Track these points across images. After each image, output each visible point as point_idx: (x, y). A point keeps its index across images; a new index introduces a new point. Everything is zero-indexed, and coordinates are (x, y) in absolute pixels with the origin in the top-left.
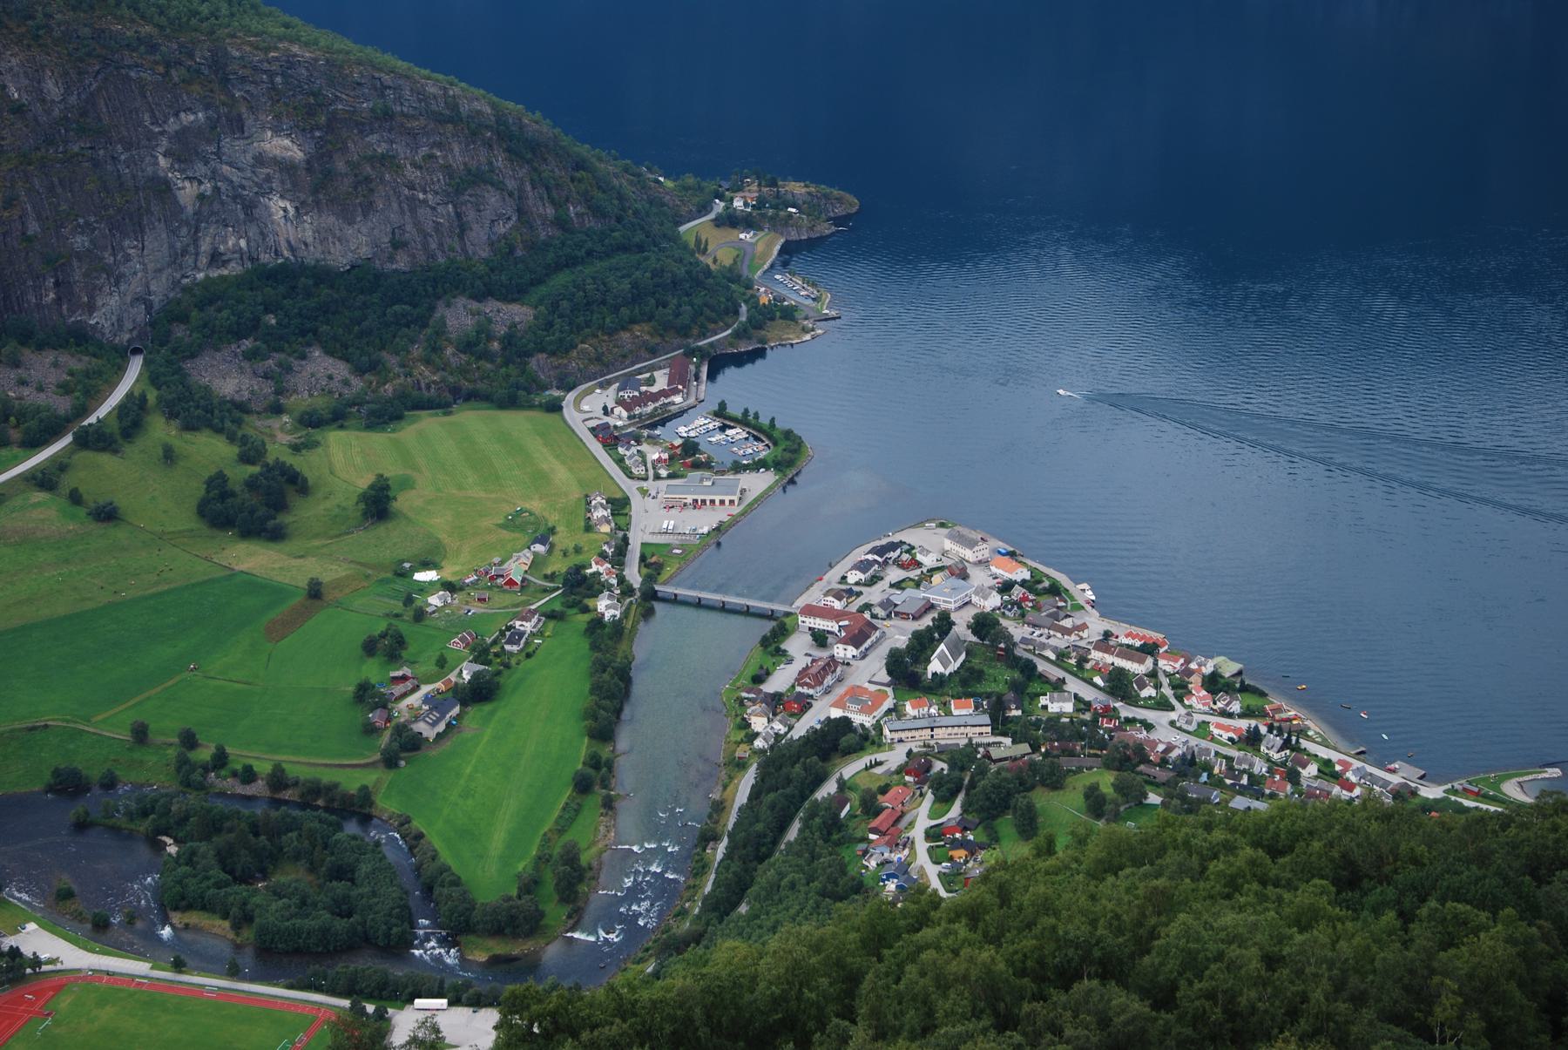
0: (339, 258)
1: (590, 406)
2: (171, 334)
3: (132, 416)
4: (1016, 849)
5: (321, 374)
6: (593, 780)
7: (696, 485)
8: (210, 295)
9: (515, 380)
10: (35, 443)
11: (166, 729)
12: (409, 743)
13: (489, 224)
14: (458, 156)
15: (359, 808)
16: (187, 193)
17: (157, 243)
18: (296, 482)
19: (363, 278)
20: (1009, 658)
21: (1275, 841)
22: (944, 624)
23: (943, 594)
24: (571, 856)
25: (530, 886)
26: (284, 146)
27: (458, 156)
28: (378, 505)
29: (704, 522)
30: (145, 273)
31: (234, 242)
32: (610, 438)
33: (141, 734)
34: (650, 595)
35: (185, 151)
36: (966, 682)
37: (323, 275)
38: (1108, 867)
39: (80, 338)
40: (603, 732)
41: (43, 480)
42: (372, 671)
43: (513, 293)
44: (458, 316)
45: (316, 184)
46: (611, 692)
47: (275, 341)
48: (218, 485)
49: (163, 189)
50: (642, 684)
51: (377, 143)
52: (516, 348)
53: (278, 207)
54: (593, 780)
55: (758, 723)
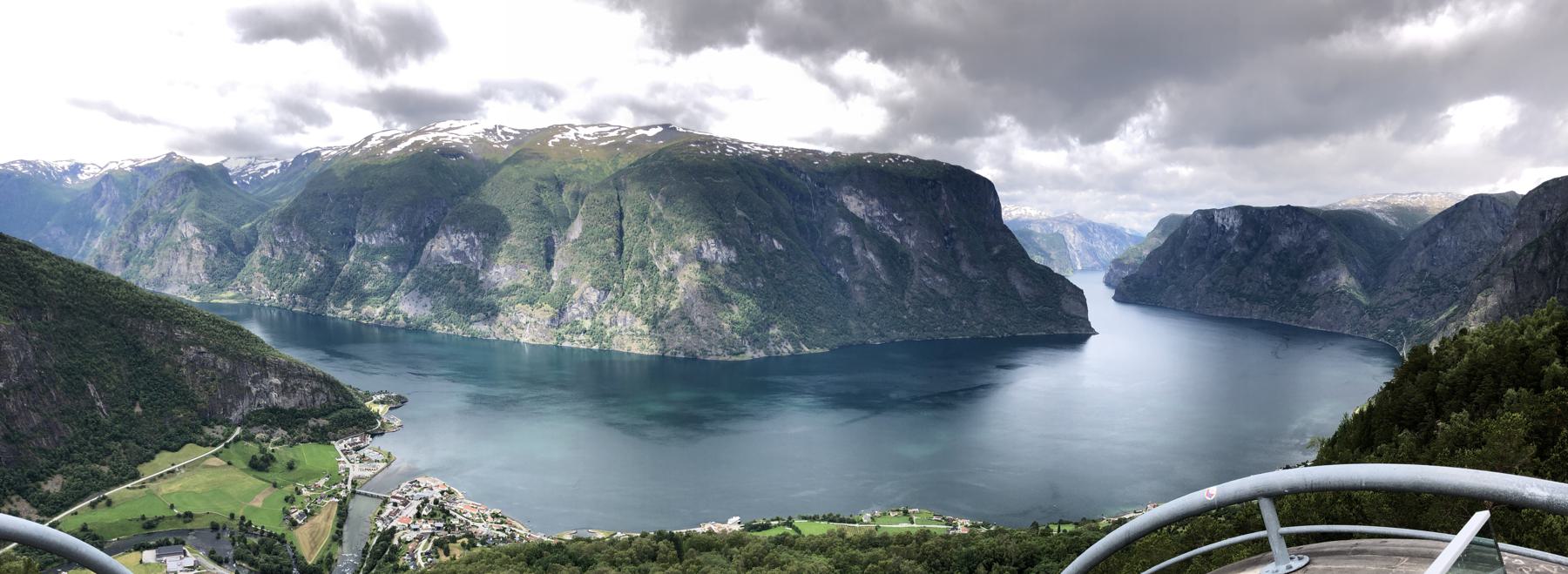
0: (287, 407)
1: (339, 446)
2: (245, 422)
3: (237, 440)
4: (443, 558)
5: (281, 433)
6: (337, 538)
7: (365, 465)
8: (257, 413)
9: (322, 437)
10: (215, 446)
11: (239, 514)
12: (294, 524)
13: (321, 400)
14: (315, 385)
15: (282, 539)
16: (254, 390)
17: (247, 402)
18: (272, 458)
19: (293, 410)
20: (443, 510)
21: (512, 553)
22: (427, 501)
23: (426, 493)
24: (330, 556)
25: (320, 562)
26: (276, 381)
27: (315, 385)
28: (291, 467)
29: (368, 474)
30: (243, 408)
31: (263, 402)
32: (346, 453)
33: (232, 516)
34: (354, 492)
35: (254, 381)
36: (433, 515)
37: (282, 411)
38: (469, 562)
39: (226, 423)
40: (340, 525)
41: (216, 455)
42: (288, 506)
43: (325, 415)
44: (311, 423)
45: (284, 390)
46: (343, 514)
47: (270, 425)
48: (254, 458)
49: (249, 389)
50: (351, 514)
51: (297, 381)
52: (324, 430)
53: (274, 394)
54: (337, 538)
55: (379, 524)
